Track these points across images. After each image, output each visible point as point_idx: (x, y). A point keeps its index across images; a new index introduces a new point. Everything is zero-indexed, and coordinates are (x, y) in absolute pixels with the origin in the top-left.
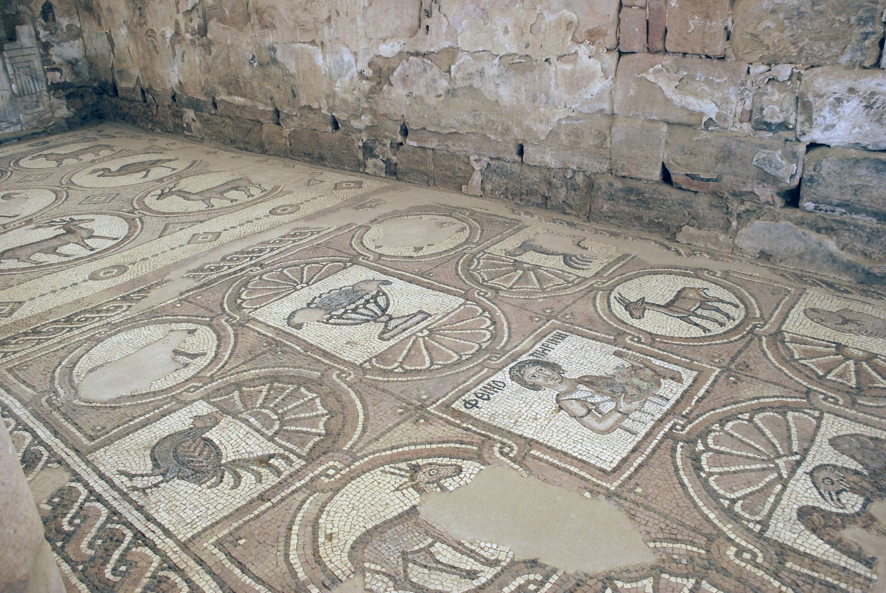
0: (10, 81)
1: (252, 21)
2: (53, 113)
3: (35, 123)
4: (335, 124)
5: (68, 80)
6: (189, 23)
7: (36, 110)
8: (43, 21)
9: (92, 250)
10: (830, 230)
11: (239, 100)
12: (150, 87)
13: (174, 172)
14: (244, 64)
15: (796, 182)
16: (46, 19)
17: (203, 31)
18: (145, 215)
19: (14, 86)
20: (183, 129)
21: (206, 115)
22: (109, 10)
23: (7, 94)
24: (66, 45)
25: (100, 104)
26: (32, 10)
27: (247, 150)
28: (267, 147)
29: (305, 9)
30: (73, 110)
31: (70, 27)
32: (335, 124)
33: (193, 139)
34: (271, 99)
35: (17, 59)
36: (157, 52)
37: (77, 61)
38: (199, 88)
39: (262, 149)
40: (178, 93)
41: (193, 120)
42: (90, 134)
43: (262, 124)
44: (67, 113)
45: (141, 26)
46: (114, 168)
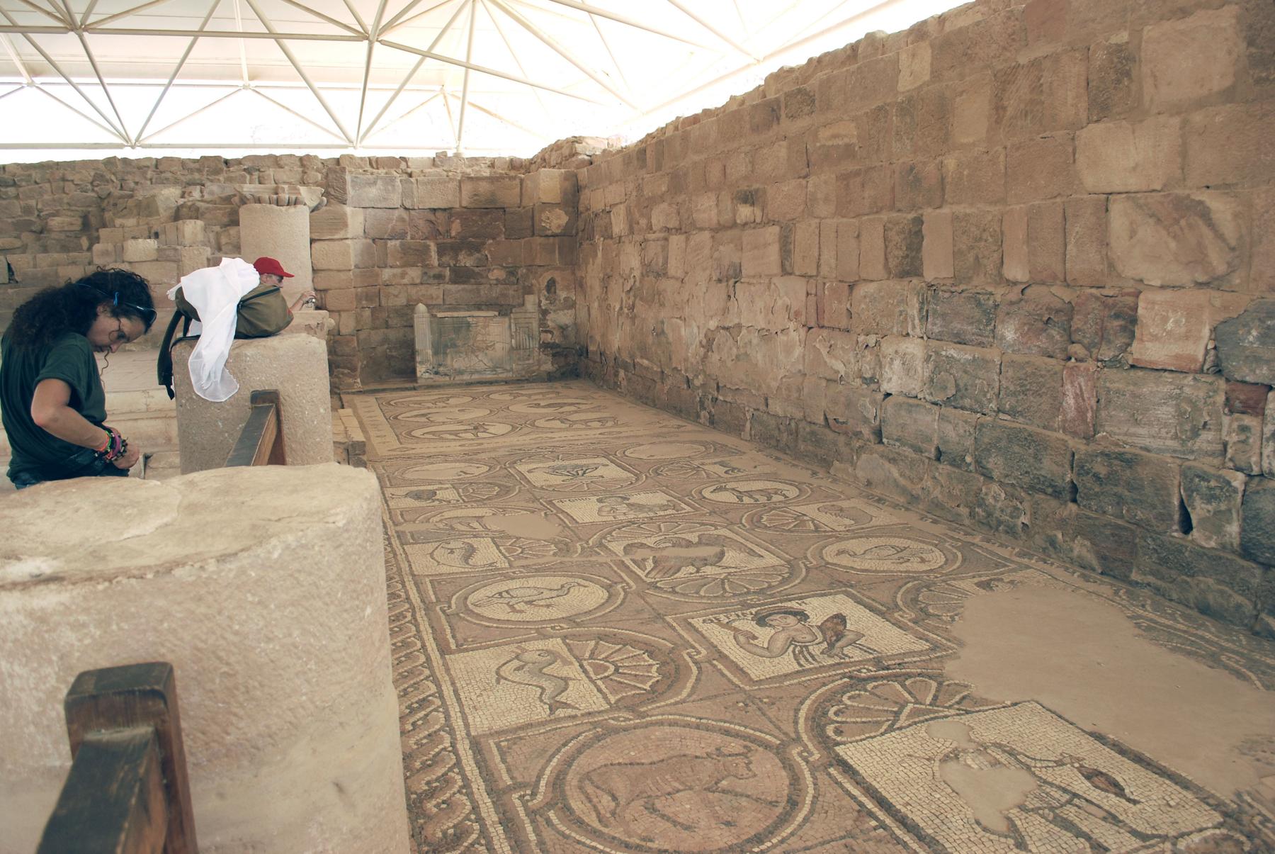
0: (512, 337)
10: (893, 461)
11: (646, 362)
16: (549, 291)
23: (507, 346)
24: (561, 313)
25: (572, 363)
31: (566, 299)
37: (567, 326)
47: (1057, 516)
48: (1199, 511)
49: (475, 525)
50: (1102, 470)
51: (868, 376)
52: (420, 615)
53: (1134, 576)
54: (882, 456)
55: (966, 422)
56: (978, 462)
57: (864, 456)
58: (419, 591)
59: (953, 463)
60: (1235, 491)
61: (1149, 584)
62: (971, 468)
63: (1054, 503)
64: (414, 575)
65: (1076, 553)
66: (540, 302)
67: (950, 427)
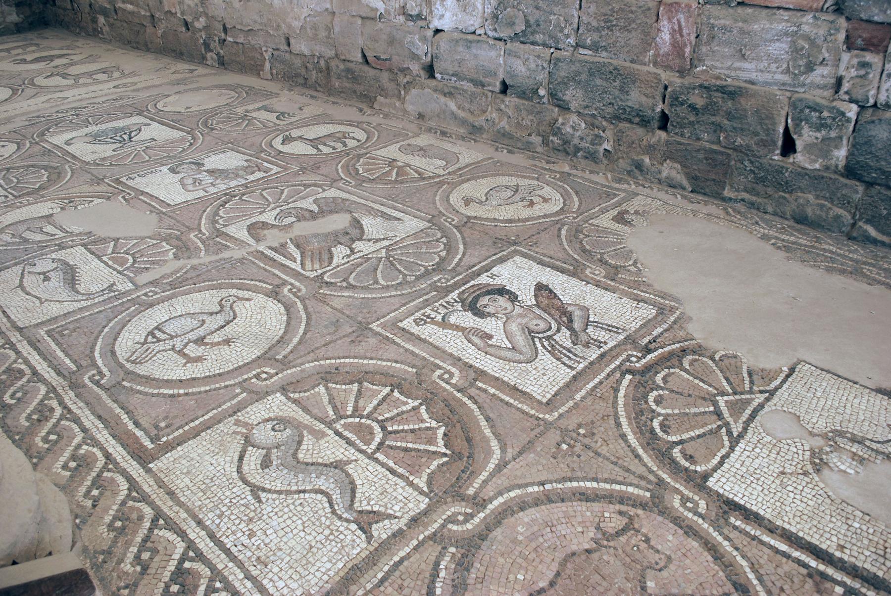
10: (449, 95)
15: (429, 59)
20: (99, 32)
27: (137, 48)
28: (150, 46)
32: (186, 24)
46: (29, 59)
47: (645, 143)
48: (805, 137)
49: (49, 229)
50: (699, 101)
51: (414, 13)
52: (69, 397)
53: (727, 193)
54: (435, 91)
55: (538, 57)
56: (552, 95)
57: (414, 92)
58: (40, 353)
59: (522, 95)
60: (848, 120)
61: (743, 200)
62: (545, 100)
63: (640, 131)
64: (20, 330)
65: (664, 174)
67: (519, 62)
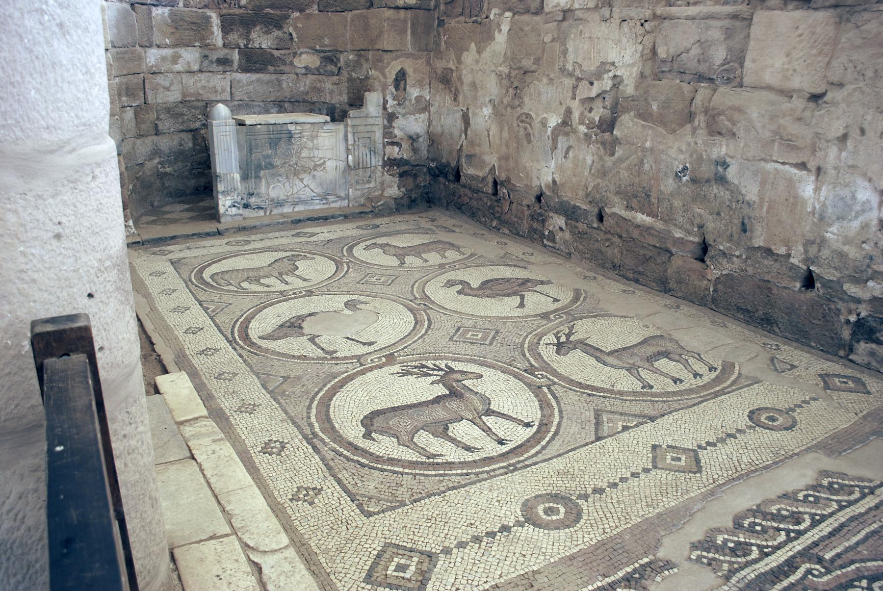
1: (696, 123)
2: (383, 191)
3: (362, 201)
4: (809, 281)
5: (405, 157)
6: (586, 113)
7: (367, 186)
8: (394, 90)
9: (501, 442)
11: (642, 218)
12: (508, 180)
13: (557, 305)
14: (666, 175)
16: (397, 87)
17: (607, 125)
18: (555, 383)
19: (350, 157)
21: (582, 226)
22: (474, 86)
24: (411, 118)
25: (436, 187)
26: (385, 77)
27: (637, 281)
28: (672, 285)
29: (799, 119)
30: (403, 189)
31: (419, 99)
32: (809, 281)
33: (555, 251)
34: (701, 227)
35: (360, 128)
36: (529, 142)
37: (418, 137)
38: (581, 193)
39: (664, 286)
40: (548, 193)
41: (561, 229)
42: (424, 223)
43: (672, 255)
44: (397, 192)
45: (513, 108)
66: (385, 102)
